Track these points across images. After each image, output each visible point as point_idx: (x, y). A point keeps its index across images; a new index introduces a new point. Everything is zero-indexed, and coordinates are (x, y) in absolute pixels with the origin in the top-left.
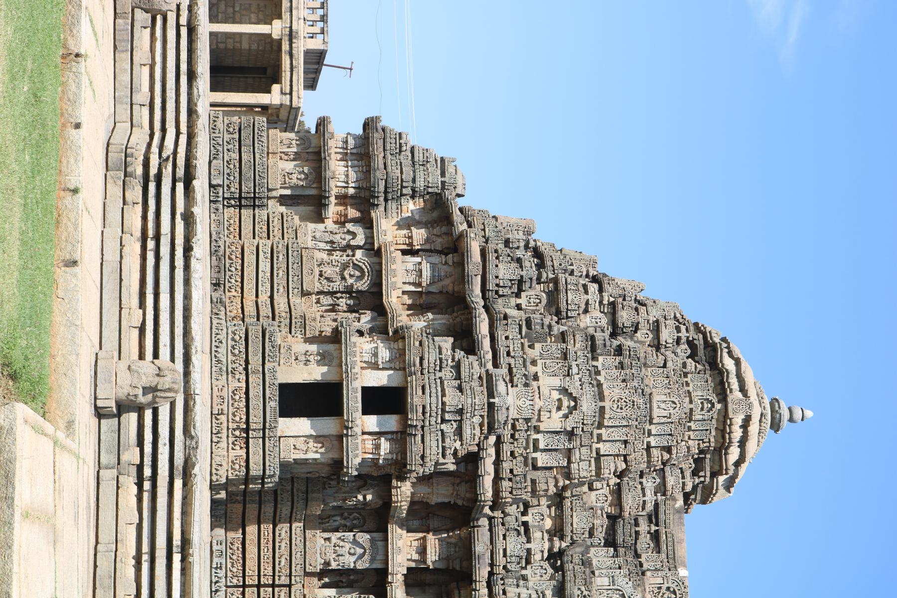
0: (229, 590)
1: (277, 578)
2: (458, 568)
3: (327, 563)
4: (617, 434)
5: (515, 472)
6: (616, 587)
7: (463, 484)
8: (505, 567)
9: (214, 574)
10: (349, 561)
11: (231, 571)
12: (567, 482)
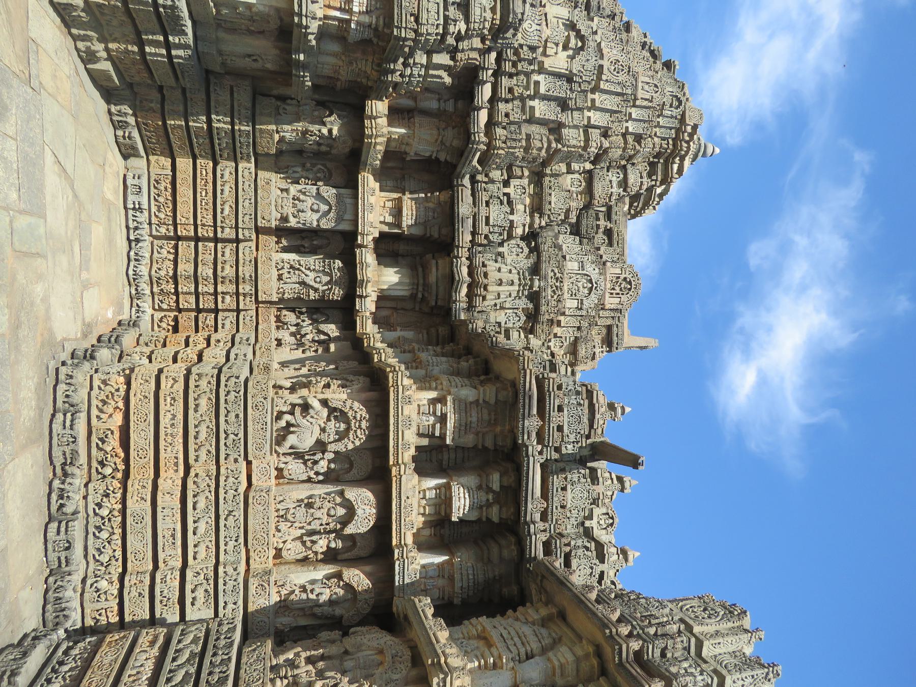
0: (156, 242)
1: (219, 230)
2: (436, 235)
3: (285, 219)
4: (610, 102)
5: (512, 118)
6: (584, 272)
7: (450, 129)
8: (486, 237)
9: (130, 217)
10: (311, 219)
11: (157, 216)
12: (560, 146)
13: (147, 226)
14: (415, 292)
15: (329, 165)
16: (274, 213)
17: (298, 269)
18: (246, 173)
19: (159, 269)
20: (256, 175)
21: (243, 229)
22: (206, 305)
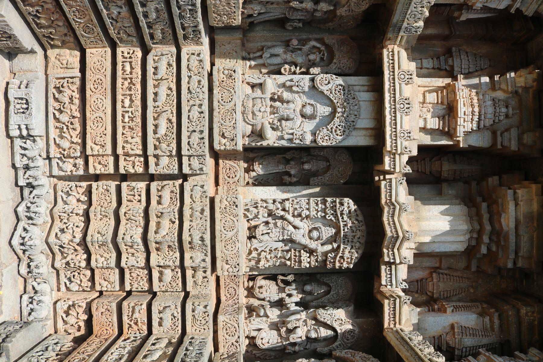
1: (152, 161)
2: (514, 146)
3: (259, 134)
9: (17, 149)
10: (303, 132)
11: (58, 146)
13: (41, 163)
14: (474, 243)
15: (329, 39)
16: (241, 124)
17: (282, 218)
18: (194, 63)
19: (62, 231)
20: (213, 64)
21: (190, 156)
22: (135, 286)
